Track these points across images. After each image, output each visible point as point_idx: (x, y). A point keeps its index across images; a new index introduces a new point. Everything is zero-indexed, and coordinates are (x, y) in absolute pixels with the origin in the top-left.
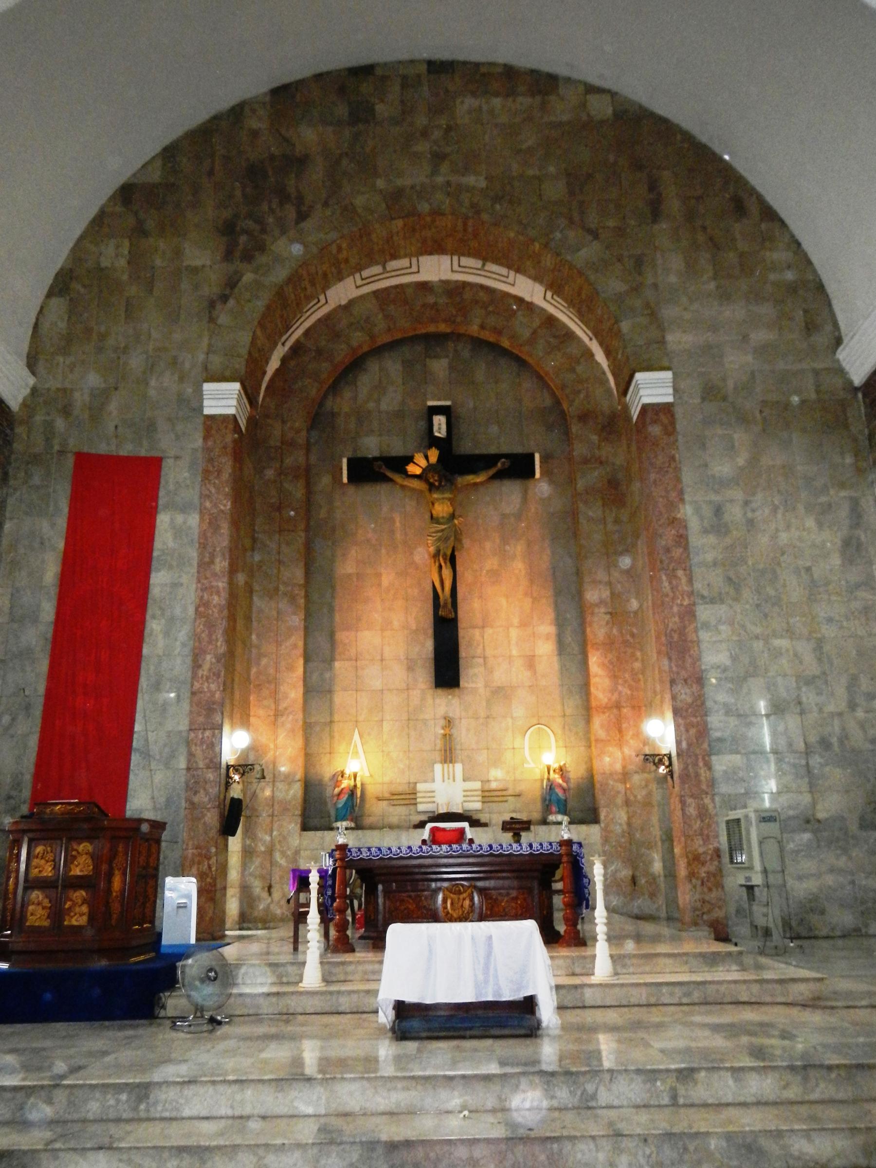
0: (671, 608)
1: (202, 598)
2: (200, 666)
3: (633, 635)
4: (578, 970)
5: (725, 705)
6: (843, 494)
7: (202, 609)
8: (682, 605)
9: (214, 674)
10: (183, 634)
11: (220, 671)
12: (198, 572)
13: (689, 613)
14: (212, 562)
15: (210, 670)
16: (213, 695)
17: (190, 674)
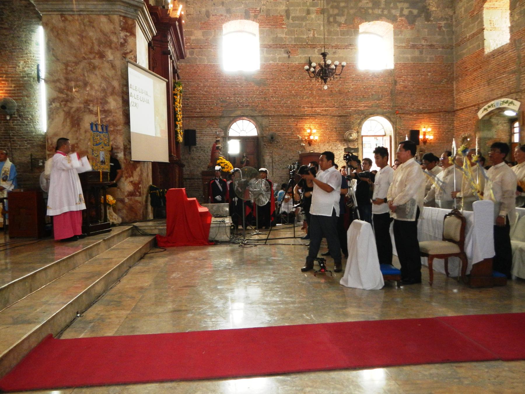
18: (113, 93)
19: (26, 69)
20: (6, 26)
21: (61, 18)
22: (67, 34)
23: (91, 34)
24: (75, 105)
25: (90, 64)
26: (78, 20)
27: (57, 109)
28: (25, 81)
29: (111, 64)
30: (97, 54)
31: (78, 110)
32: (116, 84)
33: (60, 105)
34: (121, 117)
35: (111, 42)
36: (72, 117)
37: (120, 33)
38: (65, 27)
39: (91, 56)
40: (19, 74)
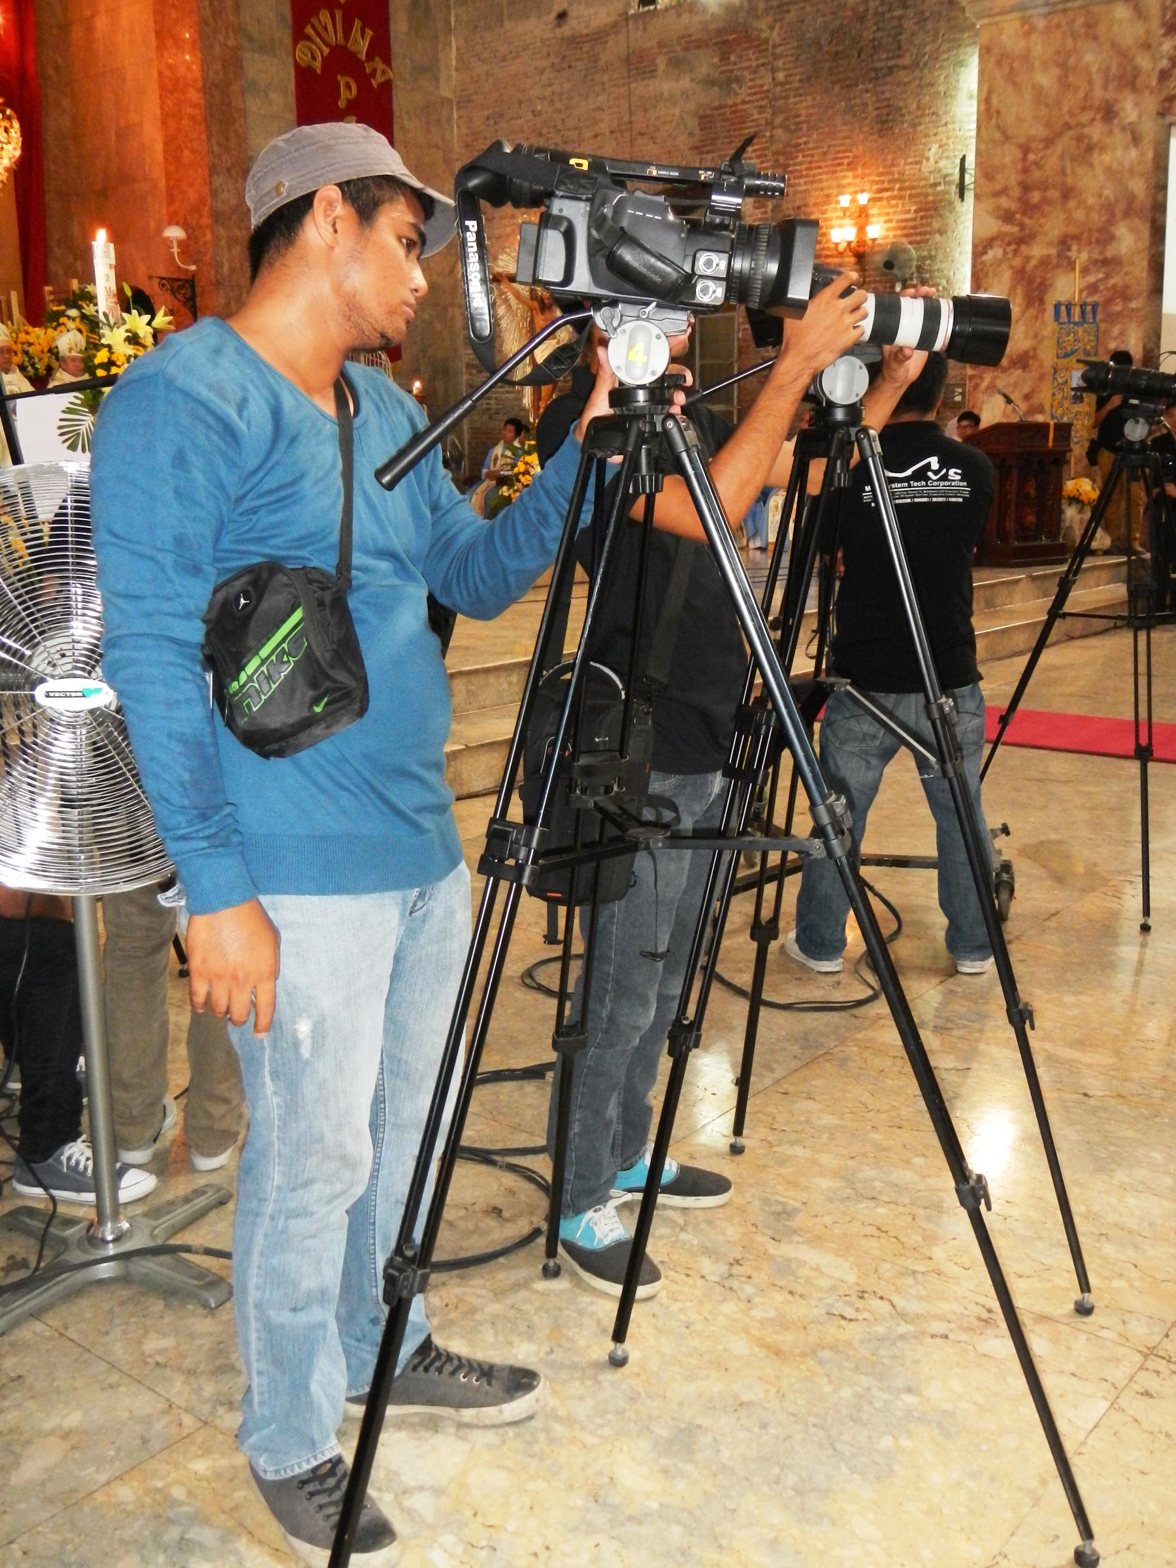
0: (212, 46)
3: (57, 68)
8: (226, 45)
13: (233, 62)
18: (1128, 213)
19: (942, 164)
20: (907, 61)
21: (1023, 25)
22: (1031, 69)
23: (1089, 58)
24: (1037, 251)
25: (1080, 139)
26: (1058, 26)
27: (998, 263)
28: (938, 194)
29: (1133, 133)
30: (1098, 110)
31: (1044, 262)
32: (1138, 186)
33: (1005, 253)
34: (1145, 275)
35: (1137, 73)
36: (1030, 282)
37: (1160, 44)
38: (1028, 50)
39: (1085, 118)
40: (927, 179)
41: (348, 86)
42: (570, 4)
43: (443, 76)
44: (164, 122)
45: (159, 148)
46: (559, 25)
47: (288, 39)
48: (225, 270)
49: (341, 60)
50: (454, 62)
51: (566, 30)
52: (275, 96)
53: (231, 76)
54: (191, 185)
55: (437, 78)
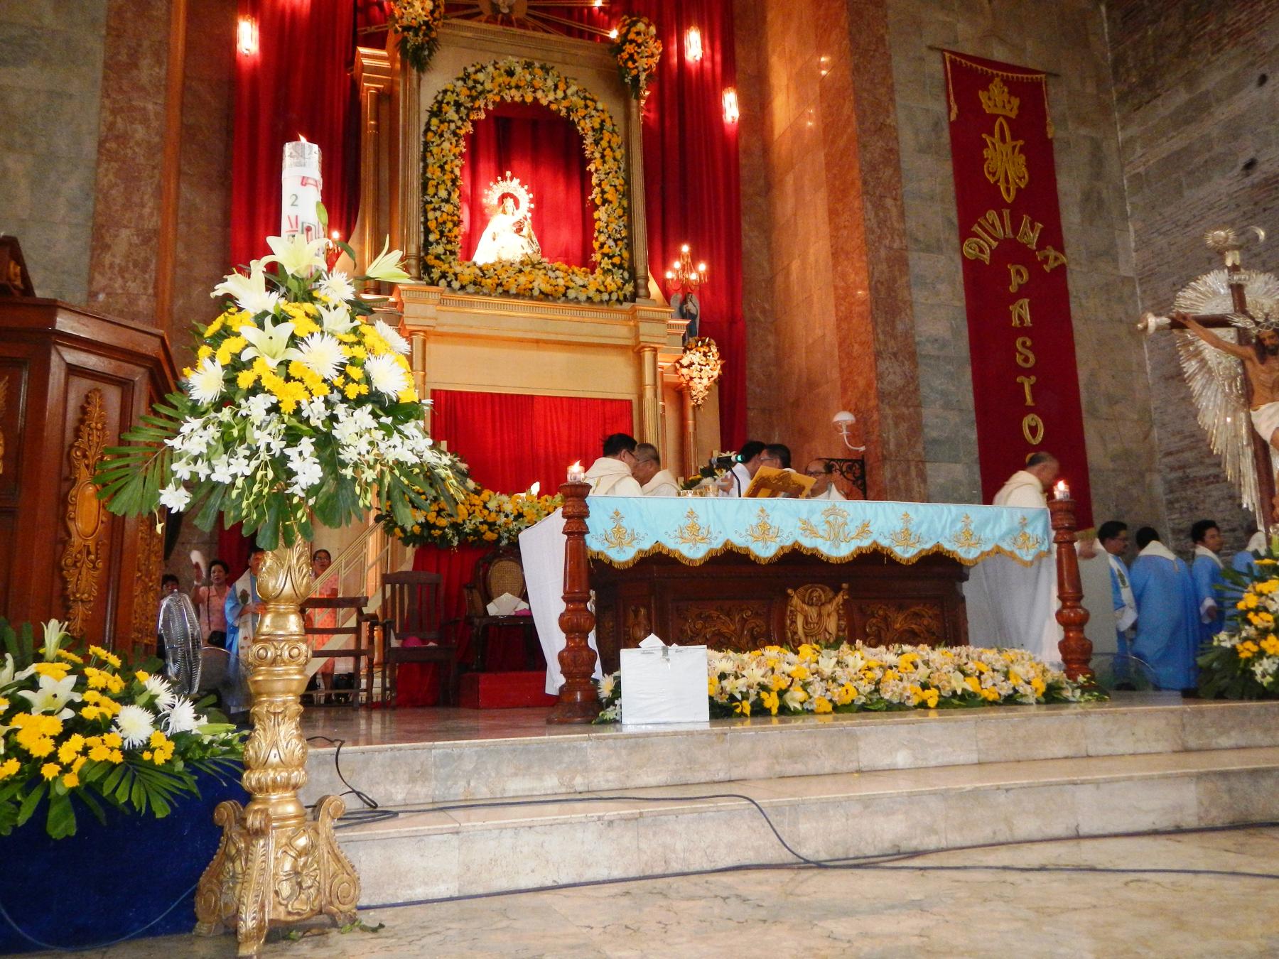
1: (111, 126)
2: (108, 247)
3: (764, 312)
4: (1193, 742)
5: (944, 394)
6: (1083, 131)
7: (112, 145)
8: (891, 248)
9: (135, 266)
10: (73, 185)
11: (147, 260)
12: (105, 78)
13: (899, 262)
14: (133, 64)
15: (128, 256)
16: (132, 300)
17: (86, 259)
41: (1019, 273)
42: (1258, 151)
43: (1122, 258)
44: (838, 327)
45: (836, 353)
46: (1248, 175)
47: (955, 240)
48: (892, 446)
49: (1010, 251)
50: (1133, 245)
51: (1256, 176)
52: (942, 287)
53: (897, 273)
54: (860, 374)
55: (1115, 260)
